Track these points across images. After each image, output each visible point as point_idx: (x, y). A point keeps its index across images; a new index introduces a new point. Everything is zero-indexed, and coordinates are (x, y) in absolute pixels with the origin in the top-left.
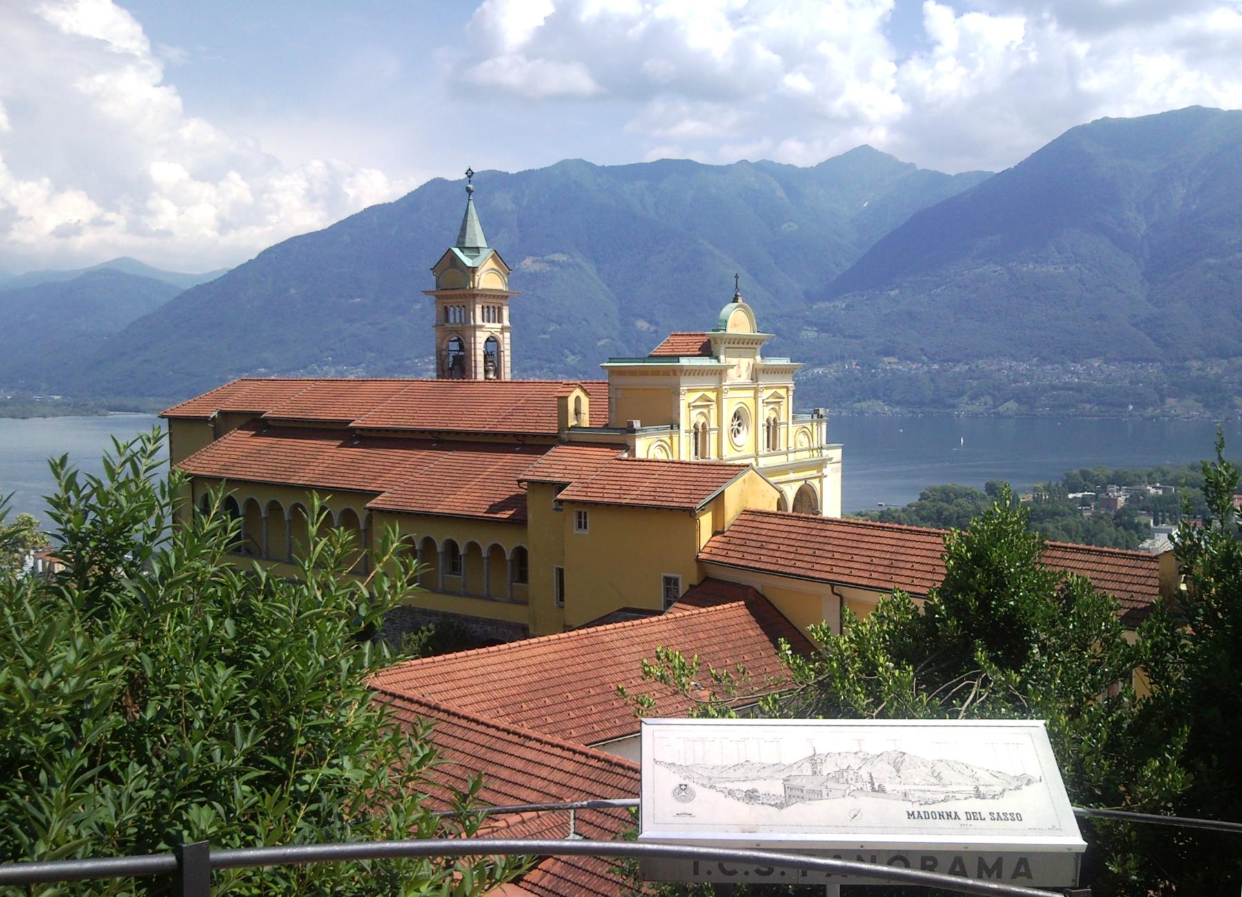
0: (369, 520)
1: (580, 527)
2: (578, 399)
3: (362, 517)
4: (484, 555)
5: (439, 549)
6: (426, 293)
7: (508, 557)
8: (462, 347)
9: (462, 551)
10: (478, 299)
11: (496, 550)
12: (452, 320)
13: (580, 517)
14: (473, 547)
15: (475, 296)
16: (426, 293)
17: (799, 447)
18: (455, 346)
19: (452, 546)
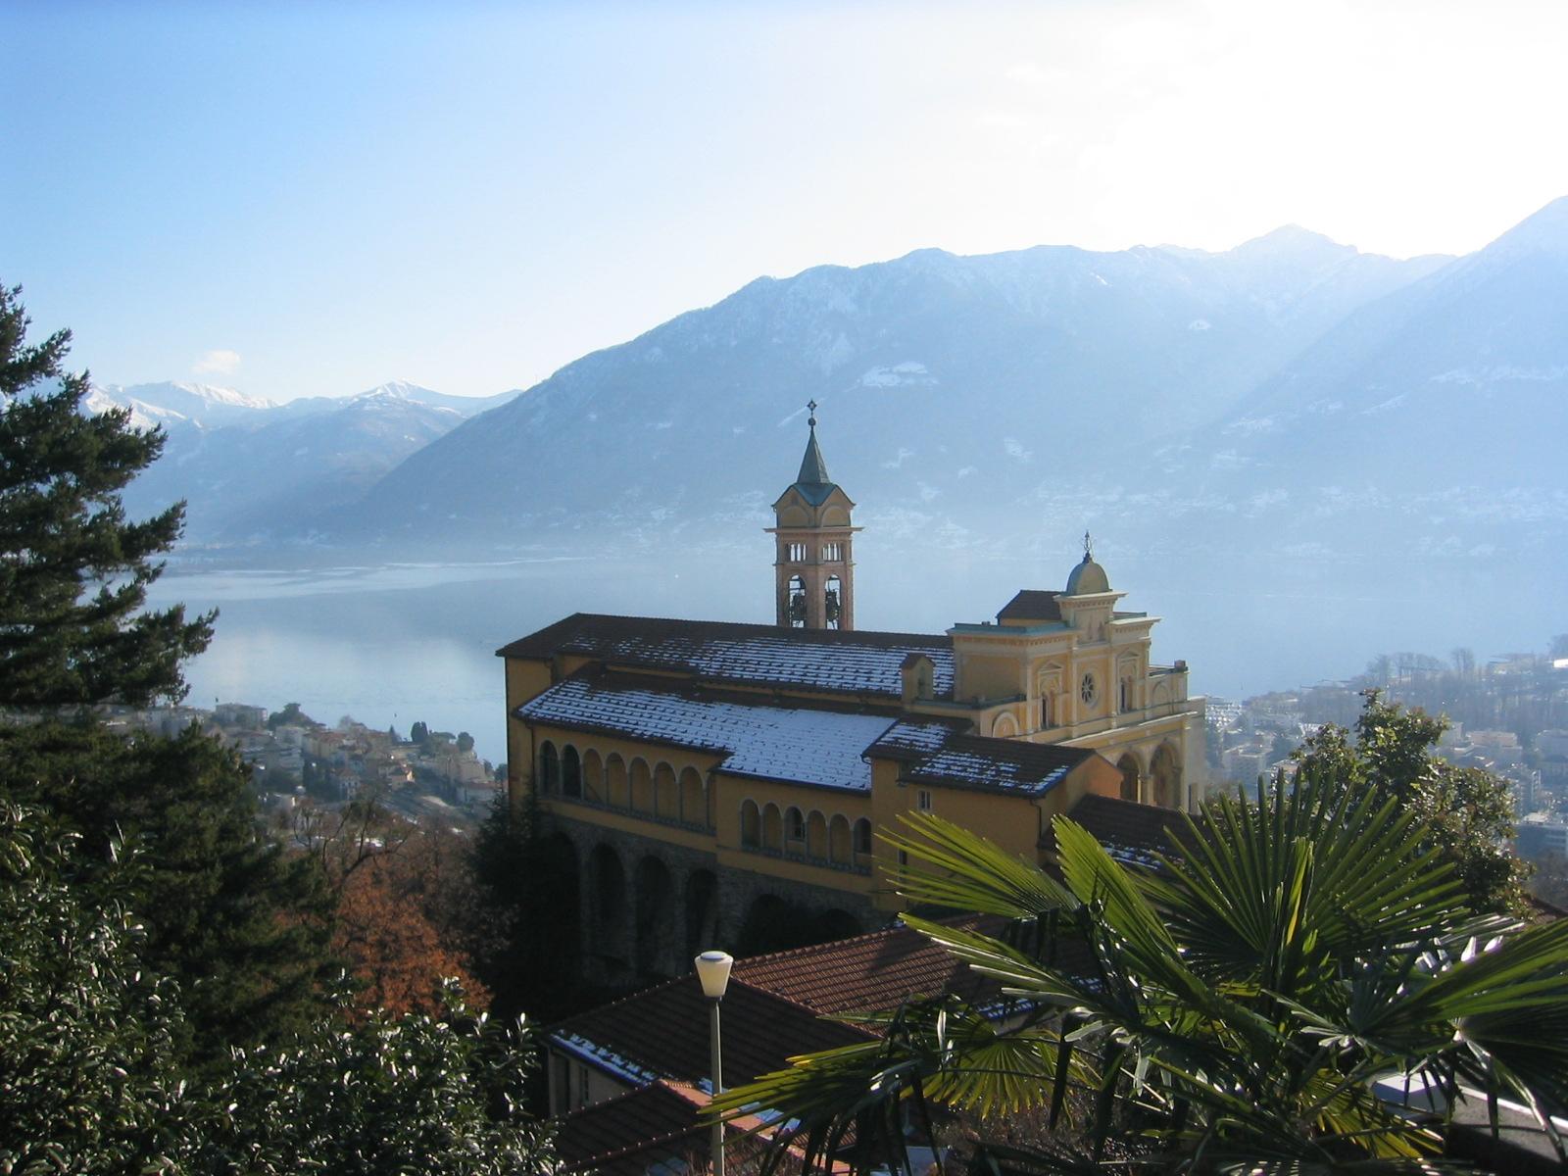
0: (711, 781)
1: (923, 806)
2: (923, 669)
3: (704, 777)
4: (827, 824)
5: (782, 814)
6: (768, 530)
7: (852, 828)
8: (803, 586)
9: (805, 820)
10: (820, 539)
11: (840, 820)
12: (793, 559)
13: (923, 796)
14: (816, 816)
15: (816, 535)
16: (768, 530)
17: (1157, 703)
18: (794, 585)
19: (796, 814)
